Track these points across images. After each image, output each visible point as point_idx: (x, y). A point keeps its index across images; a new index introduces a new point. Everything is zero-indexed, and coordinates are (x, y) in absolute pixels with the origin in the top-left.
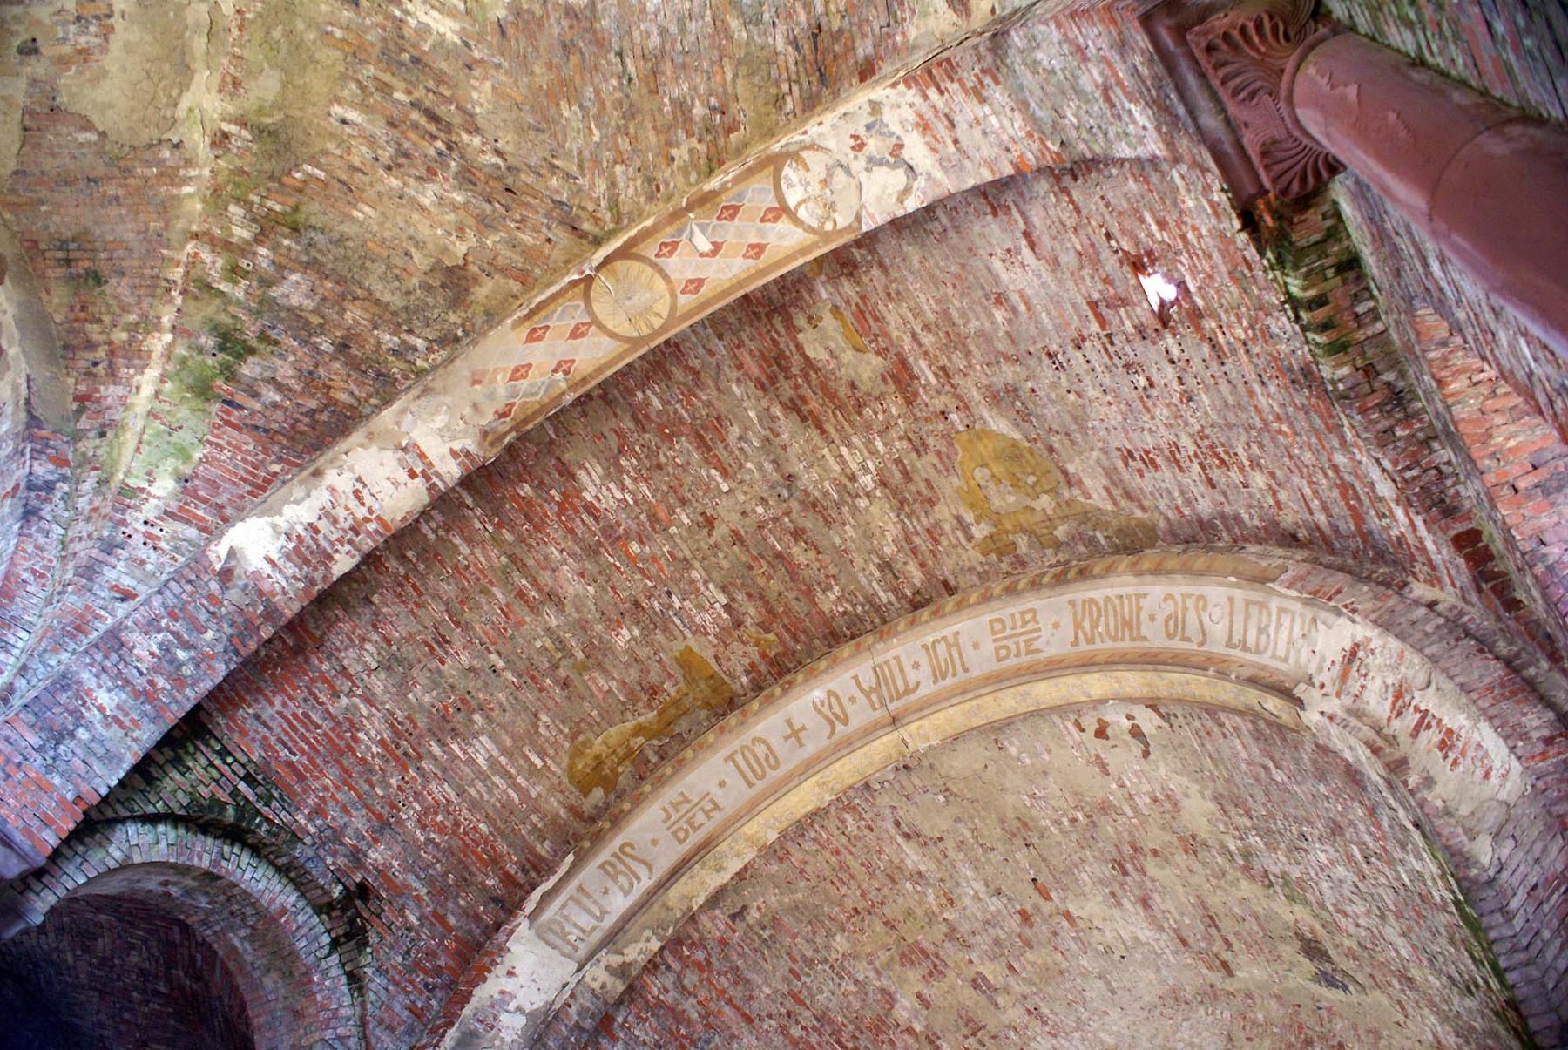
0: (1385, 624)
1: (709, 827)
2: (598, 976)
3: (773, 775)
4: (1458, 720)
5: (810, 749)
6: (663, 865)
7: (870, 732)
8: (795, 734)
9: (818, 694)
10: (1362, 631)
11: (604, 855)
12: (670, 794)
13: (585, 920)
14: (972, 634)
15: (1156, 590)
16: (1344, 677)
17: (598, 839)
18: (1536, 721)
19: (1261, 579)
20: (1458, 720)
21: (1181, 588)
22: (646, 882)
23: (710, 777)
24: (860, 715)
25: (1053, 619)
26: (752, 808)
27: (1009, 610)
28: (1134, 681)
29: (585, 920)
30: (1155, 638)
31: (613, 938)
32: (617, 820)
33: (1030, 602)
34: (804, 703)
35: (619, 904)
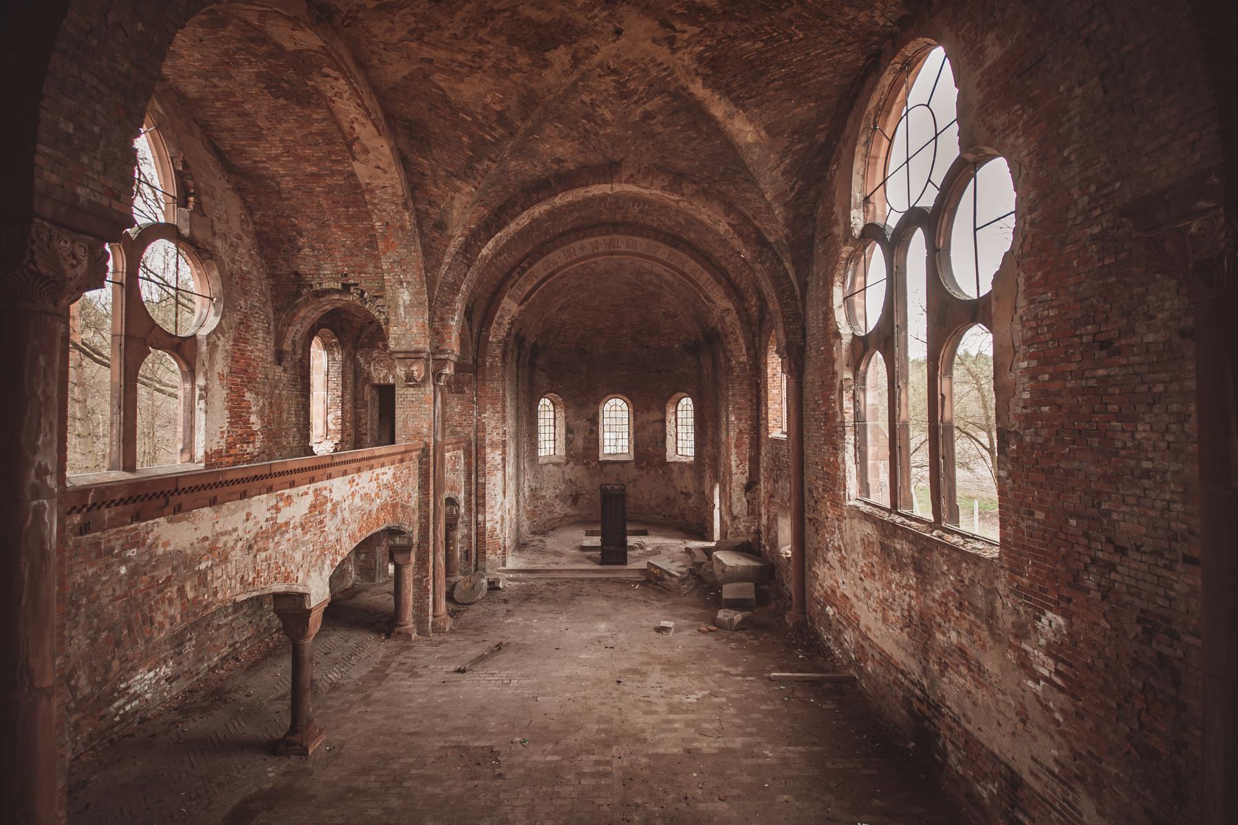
0: (738, 313)
1: (553, 268)
2: (523, 307)
4: (741, 341)
5: (586, 253)
6: (540, 278)
8: (583, 248)
10: (732, 308)
12: (545, 259)
14: (642, 244)
16: (722, 312)
17: (524, 270)
19: (719, 282)
21: (698, 266)
23: (557, 257)
24: (602, 249)
25: (664, 252)
26: (566, 266)
27: (654, 243)
30: (687, 270)
32: (530, 265)
34: (588, 242)
35: (528, 288)
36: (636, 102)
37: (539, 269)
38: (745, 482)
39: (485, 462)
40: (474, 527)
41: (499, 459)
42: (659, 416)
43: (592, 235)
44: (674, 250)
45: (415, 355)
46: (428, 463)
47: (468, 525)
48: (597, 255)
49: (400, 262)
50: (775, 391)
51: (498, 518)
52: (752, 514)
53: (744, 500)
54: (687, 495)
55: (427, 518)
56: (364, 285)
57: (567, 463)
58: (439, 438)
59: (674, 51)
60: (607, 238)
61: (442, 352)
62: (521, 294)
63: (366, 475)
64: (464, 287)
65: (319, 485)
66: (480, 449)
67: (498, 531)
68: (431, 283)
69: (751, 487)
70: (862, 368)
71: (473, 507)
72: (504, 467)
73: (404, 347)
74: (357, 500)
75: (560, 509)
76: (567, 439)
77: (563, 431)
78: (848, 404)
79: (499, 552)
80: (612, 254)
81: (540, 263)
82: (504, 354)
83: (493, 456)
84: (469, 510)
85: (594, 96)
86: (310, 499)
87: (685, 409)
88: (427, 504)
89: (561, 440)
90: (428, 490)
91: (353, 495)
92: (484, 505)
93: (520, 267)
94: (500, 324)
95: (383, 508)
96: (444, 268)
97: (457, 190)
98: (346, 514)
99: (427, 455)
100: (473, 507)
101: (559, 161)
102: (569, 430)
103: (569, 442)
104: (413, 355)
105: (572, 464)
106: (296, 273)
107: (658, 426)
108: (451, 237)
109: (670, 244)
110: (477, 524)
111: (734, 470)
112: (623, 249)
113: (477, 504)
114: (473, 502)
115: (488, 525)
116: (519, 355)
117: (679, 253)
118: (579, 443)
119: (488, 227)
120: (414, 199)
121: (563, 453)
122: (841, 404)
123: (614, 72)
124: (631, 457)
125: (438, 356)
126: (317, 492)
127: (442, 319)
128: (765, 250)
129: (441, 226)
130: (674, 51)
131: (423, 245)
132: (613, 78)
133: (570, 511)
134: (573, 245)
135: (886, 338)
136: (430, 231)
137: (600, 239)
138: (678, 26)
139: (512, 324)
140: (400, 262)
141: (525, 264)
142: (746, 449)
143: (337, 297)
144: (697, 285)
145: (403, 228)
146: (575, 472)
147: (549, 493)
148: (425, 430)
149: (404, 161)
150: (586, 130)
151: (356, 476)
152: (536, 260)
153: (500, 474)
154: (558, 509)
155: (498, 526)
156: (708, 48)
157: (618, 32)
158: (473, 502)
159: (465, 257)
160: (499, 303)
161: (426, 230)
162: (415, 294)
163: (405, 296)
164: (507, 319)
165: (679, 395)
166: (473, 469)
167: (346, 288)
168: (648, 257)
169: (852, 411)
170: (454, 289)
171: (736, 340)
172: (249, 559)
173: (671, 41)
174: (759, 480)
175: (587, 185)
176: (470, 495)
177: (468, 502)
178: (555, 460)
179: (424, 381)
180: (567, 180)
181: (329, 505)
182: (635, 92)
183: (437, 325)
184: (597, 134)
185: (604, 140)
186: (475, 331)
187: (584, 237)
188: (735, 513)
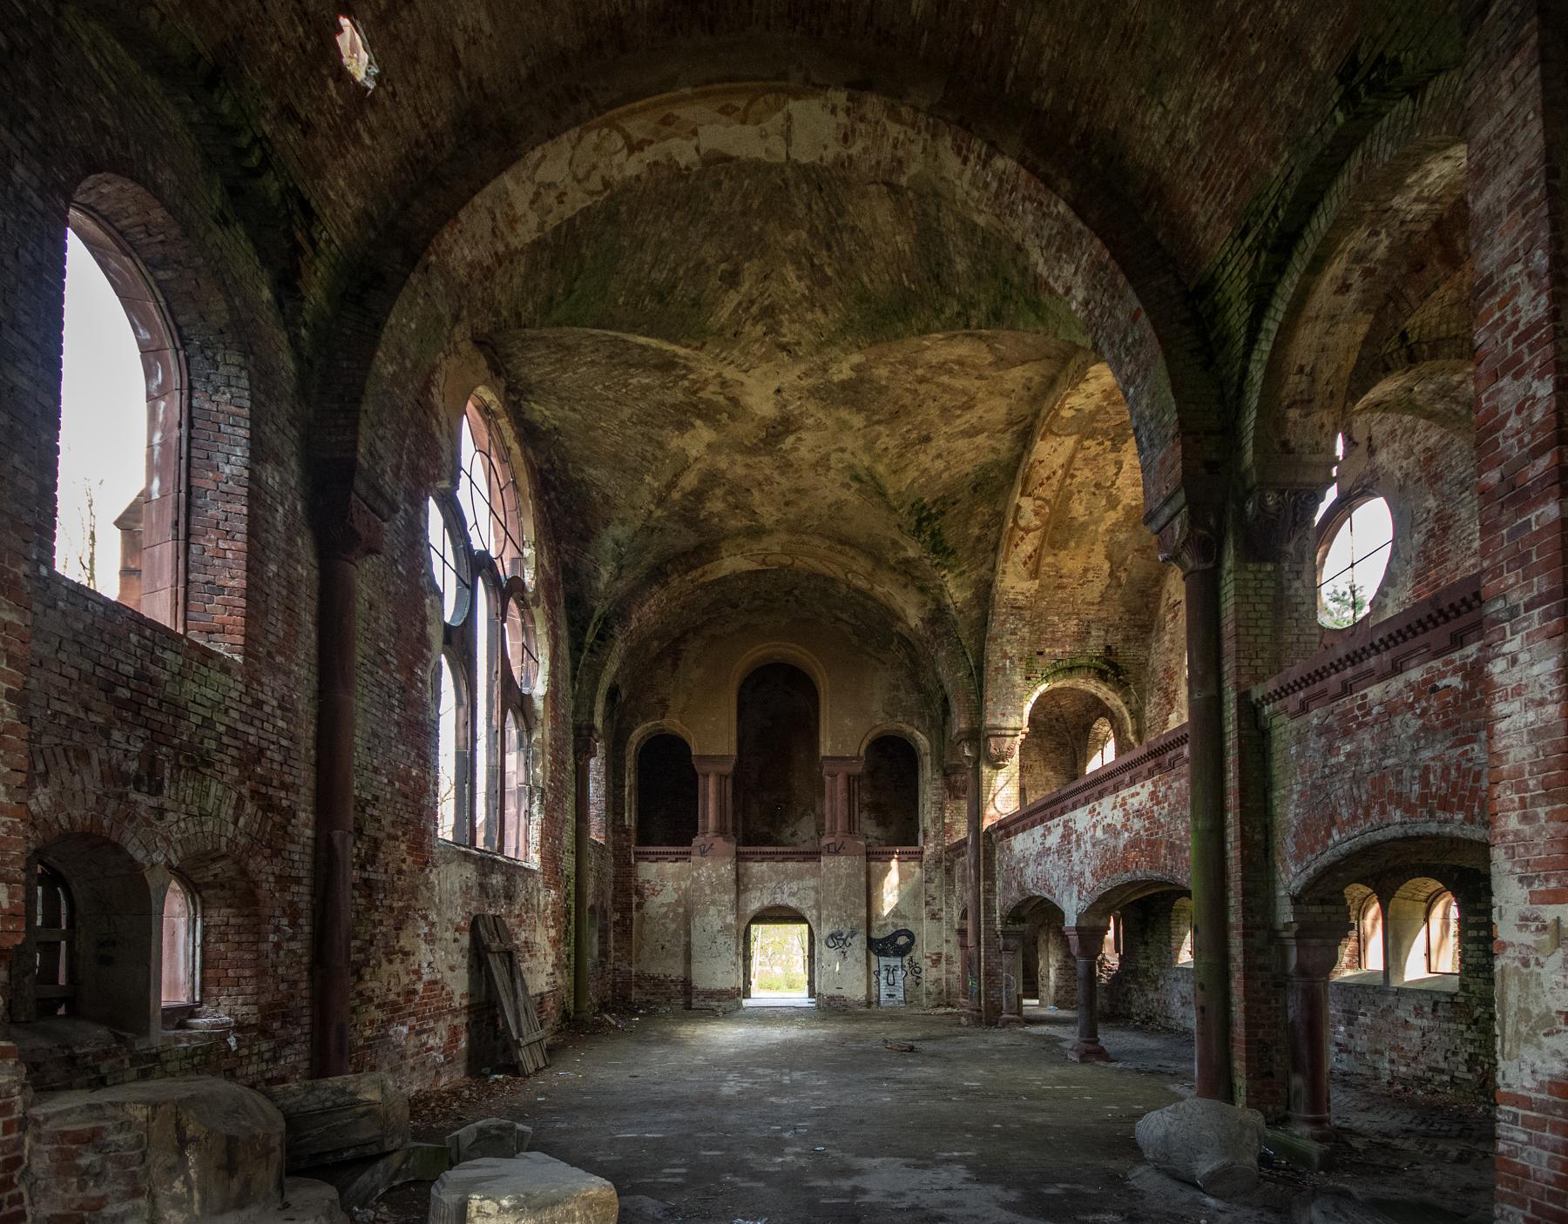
36: (752, 302)
59: (719, 375)
63: (1108, 801)
65: (1066, 817)
74: (1099, 833)
85: (809, 316)
86: (1060, 830)
91: (1095, 826)
95: (1134, 844)
98: (1089, 846)
123: (784, 348)
130: (719, 375)
132: (785, 340)
138: (721, 398)
150: (829, 248)
156: (684, 377)
157: (778, 391)
173: (724, 384)
182: (756, 320)
184: (813, 232)
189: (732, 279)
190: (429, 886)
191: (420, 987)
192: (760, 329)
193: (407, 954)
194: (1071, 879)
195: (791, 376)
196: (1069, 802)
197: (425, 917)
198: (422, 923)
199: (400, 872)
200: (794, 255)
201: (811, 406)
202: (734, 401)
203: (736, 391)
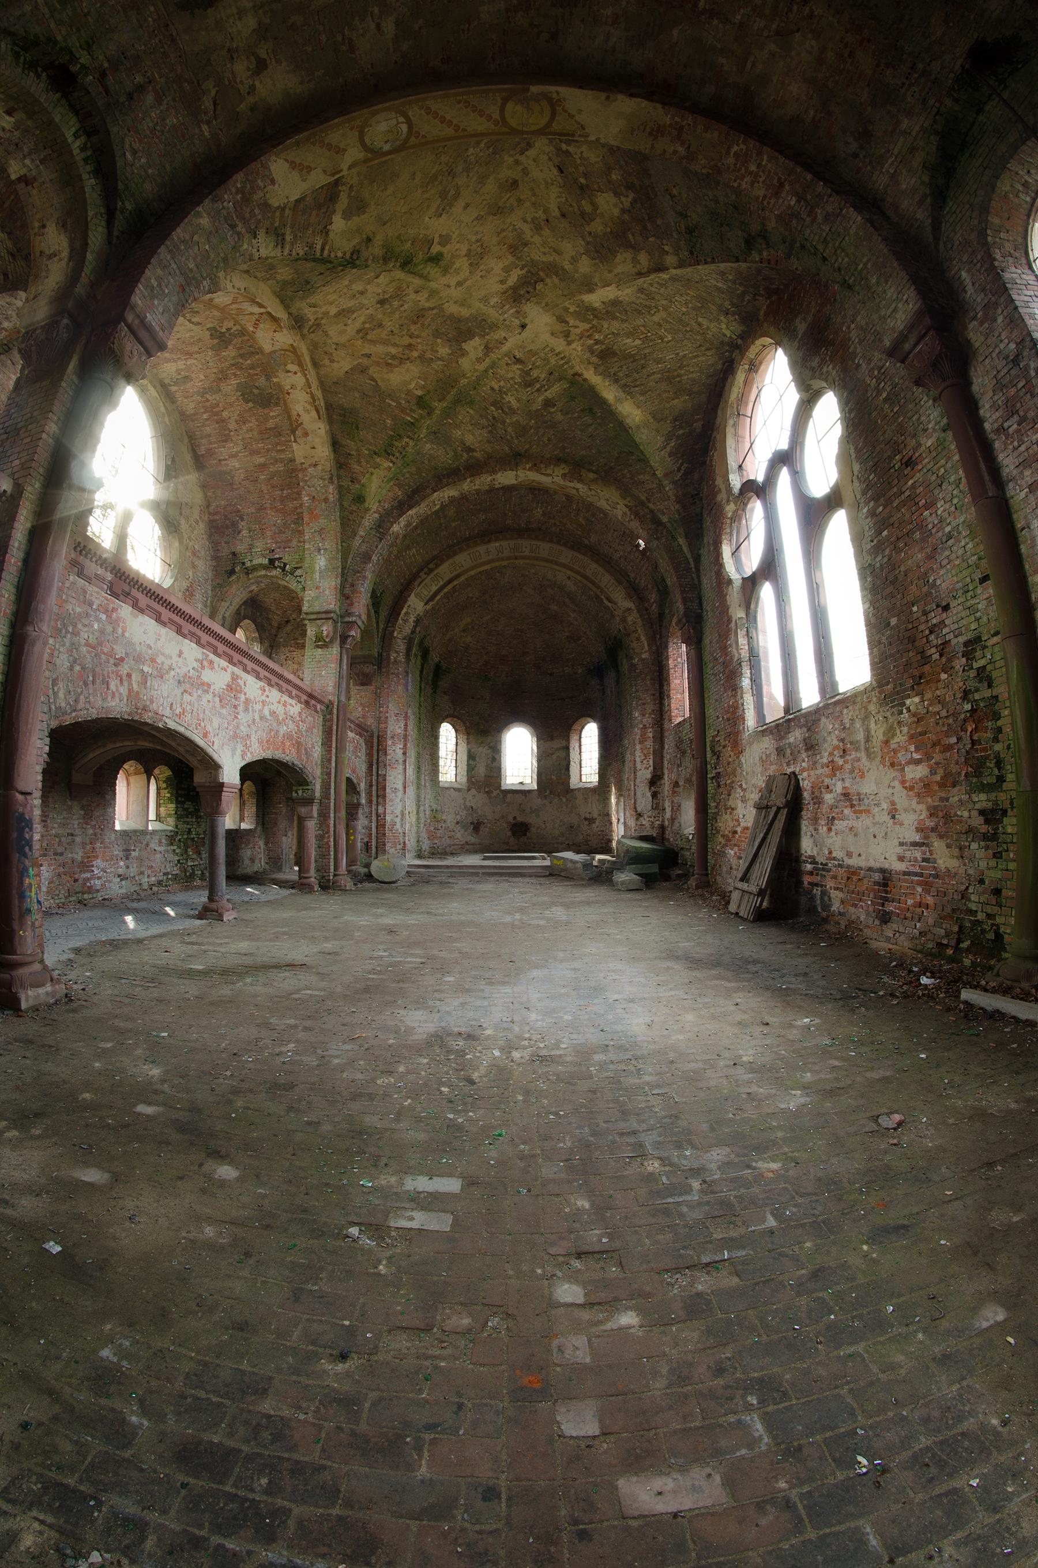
0: (639, 611)
3: (479, 561)
4: (643, 638)
5: (491, 557)
6: (446, 579)
7: (508, 558)
8: (488, 552)
9: (497, 544)
11: (432, 575)
12: (451, 561)
13: (426, 593)
14: (545, 548)
15: (594, 566)
16: (624, 612)
17: (431, 571)
18: (654, 648)
19: (620, 583)
20: (643, 638)
21: (600, 569)
22: (442, 583)
23: (463, 559)
24: (506, 553)
25: (566, 555)
28: (579, 578)
29: (426, 593)
30: (589, 573)
31: (432, 598)
32: (437, 566)
33: (563, 549)
35: (434, 588)
37: (445, 570)
38: (649, 776)
39: (386, 754)
40: (374, 818)
41: (400, 752)
42: (564, 743)
43: (497, 540)
44: (576, 554)
45: (325, 615)
46: (331, 720)
47: (369, 816)
48: (502, 559)
49: (321, 532)
50: (677, 681)
51: (398, 812)
52: (656, 808)
53: (649, 795)
54: (591, 821)
55: (329, 774)
56: (286, 558)
57: (469, 790)
58: (343, 698)
60: (512, 543)
61: (349, 614)
62: (427, 593)
64: (374, 558)
66: (381, 739)
67: (398, 826)
68: (345, 553)
69: (655, 780)
70: (752, 606)
71: (374, 799)
72: (405, 761)
73: (317, 609)
75: (462, 836)
76: (468, 765)
77: (465, 758)
78: (742, 641)
79: (400, 847)
80: (516, 558)
81: (446, 565)
82: (409, 650)
83: (395, 750)
84: (370, 802)
87: (590, 734)
88: (329, 761)
89: (463, 766)
90: (331, 747)
92: (384, 796)
93: (428, 566)
94: (406, 621)
96: (357, 541)
97: (377, 466)
98: (257, 717)
99: (331, 713)
100: (374, 799)
101: (470, 450)
102: (471, 757)
103: (471, 768)
104: (324, 616)
105: (473, 791)
106: (234, 554)
107: (562, 753)
108: (368, 509)
109: (572, 548)
110: (378, 816)
111: (639, 766)
112: (527, 554)
113: (378, 796)
114: (374, 793)
115: (388, 818)
116: (422, 666)
117: (581, 557)
118: (481, 770)
119: (402, 506)
120: (339, 477)
121: (465, 779)
122: (737, 642)
124: (535, 786)
125: (347, 619)
126: (234, 678)
127: (352, 585)
128: (660, 528)
129: (360, 499)
131: (342, 518)
133: (472, 839)
134: (478, 548)
135: (771, 567)
136: (350, 502)
137: (505, 543)
139: (418, 621)
140: (321, 532)
141: (431, 566)
142: (649, 743)
143: (263, 572)
144: (598, 587)
145: (326, 500)
146: (477, 800)
147: (450, 818)
148: (330, 689)
149: (335, 444)
151: (267, 688)
152: (442, 561)
153: (401, 767)
154: (459, 835)
155: (398, 820)
158: (374, 793)
159: (378, 531)
160: (406, 601)
161: (345, 504)
162: (329, 560)
163: (321, 562)
164: (412, 619)
165: (583, 720)
166: (375, 761)
167: (272, 561)
168: (551, 562)
169: (747, 647)
170: (366, 558)
171: (638, 639)
172: (178, 691)
174: (663, 774)
175: (494, 472)
176: (371, 786)
177: (369, 794)
178: (456, 786)
179: (331, 641)
180: (474, 468)
181: (243, 697)
183: (347, 591)
185: (510, 429)
186: (381, 626)
187: (489, 541)
188: (639, 809)
189: (548, 403)
190: (740, 764)
191: (739, 829)
192: (535, 374)
193: (733, 809)
194: (235, 736)
195: (513, 342)
196: (250, 665)
197: (741, 786)
198: (739, 790)
199: (729, 764)
200: (513, 412)
201: (493, 315)
202: (561, 320)
203: (559, 327)
